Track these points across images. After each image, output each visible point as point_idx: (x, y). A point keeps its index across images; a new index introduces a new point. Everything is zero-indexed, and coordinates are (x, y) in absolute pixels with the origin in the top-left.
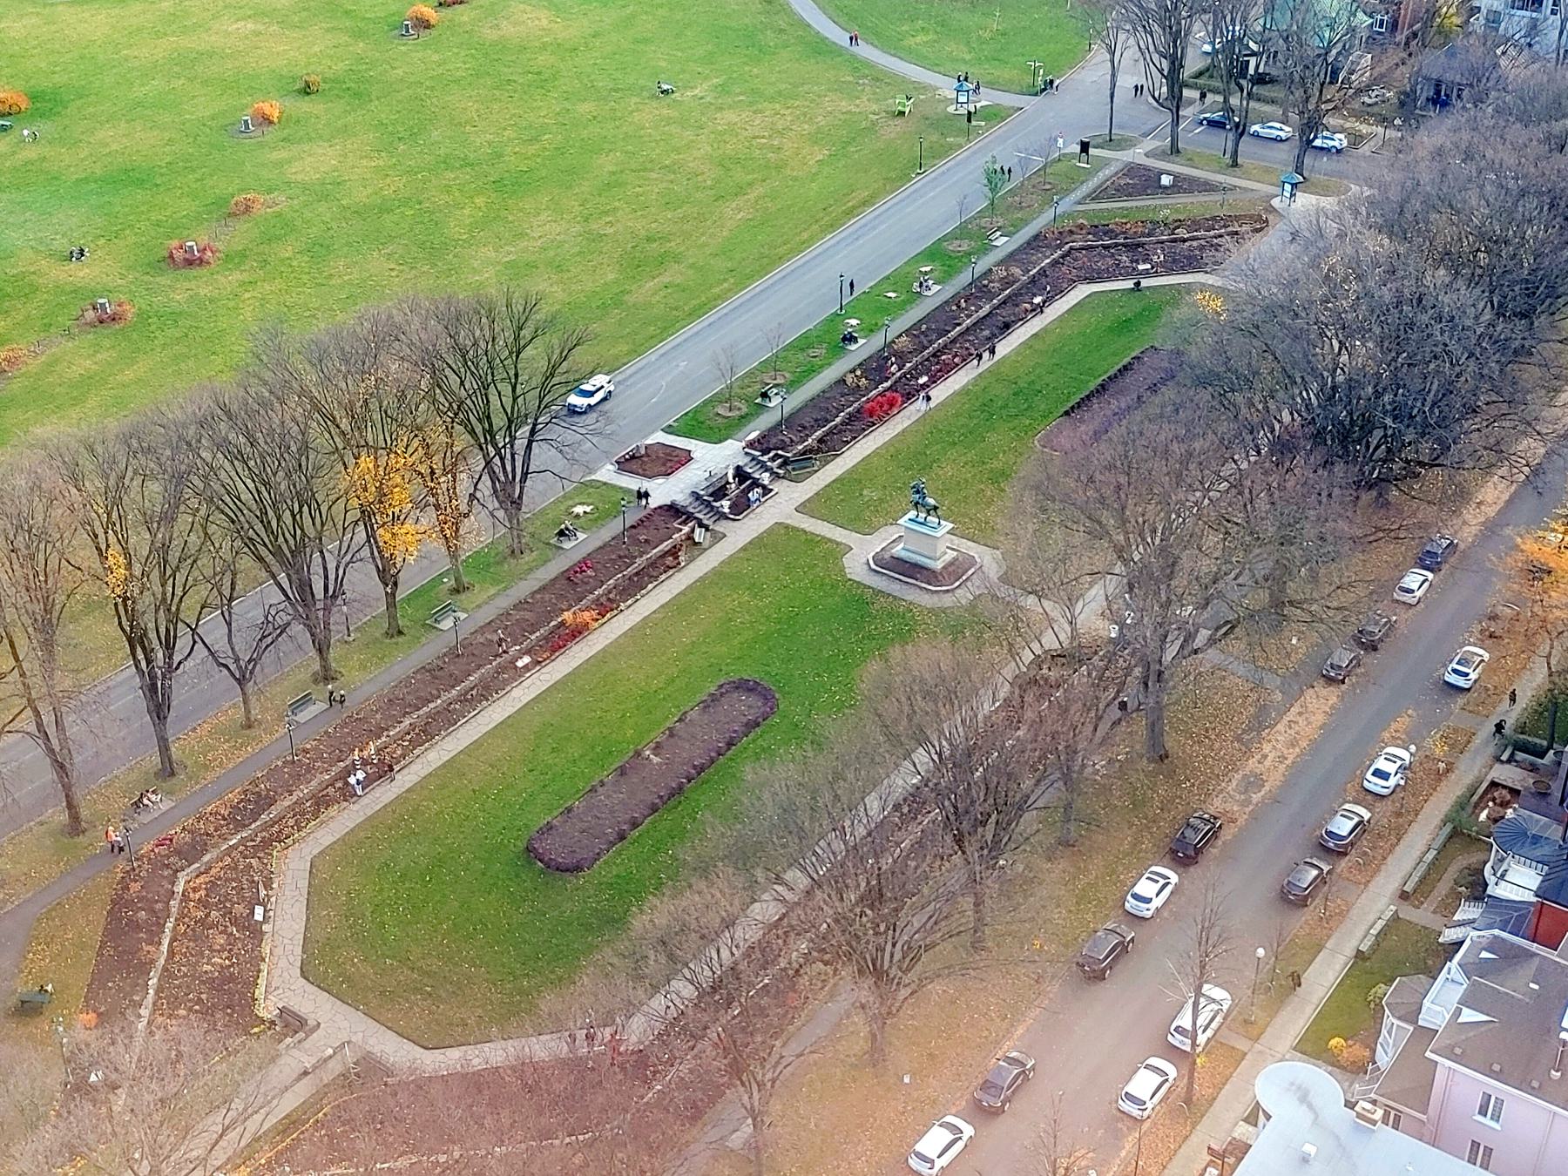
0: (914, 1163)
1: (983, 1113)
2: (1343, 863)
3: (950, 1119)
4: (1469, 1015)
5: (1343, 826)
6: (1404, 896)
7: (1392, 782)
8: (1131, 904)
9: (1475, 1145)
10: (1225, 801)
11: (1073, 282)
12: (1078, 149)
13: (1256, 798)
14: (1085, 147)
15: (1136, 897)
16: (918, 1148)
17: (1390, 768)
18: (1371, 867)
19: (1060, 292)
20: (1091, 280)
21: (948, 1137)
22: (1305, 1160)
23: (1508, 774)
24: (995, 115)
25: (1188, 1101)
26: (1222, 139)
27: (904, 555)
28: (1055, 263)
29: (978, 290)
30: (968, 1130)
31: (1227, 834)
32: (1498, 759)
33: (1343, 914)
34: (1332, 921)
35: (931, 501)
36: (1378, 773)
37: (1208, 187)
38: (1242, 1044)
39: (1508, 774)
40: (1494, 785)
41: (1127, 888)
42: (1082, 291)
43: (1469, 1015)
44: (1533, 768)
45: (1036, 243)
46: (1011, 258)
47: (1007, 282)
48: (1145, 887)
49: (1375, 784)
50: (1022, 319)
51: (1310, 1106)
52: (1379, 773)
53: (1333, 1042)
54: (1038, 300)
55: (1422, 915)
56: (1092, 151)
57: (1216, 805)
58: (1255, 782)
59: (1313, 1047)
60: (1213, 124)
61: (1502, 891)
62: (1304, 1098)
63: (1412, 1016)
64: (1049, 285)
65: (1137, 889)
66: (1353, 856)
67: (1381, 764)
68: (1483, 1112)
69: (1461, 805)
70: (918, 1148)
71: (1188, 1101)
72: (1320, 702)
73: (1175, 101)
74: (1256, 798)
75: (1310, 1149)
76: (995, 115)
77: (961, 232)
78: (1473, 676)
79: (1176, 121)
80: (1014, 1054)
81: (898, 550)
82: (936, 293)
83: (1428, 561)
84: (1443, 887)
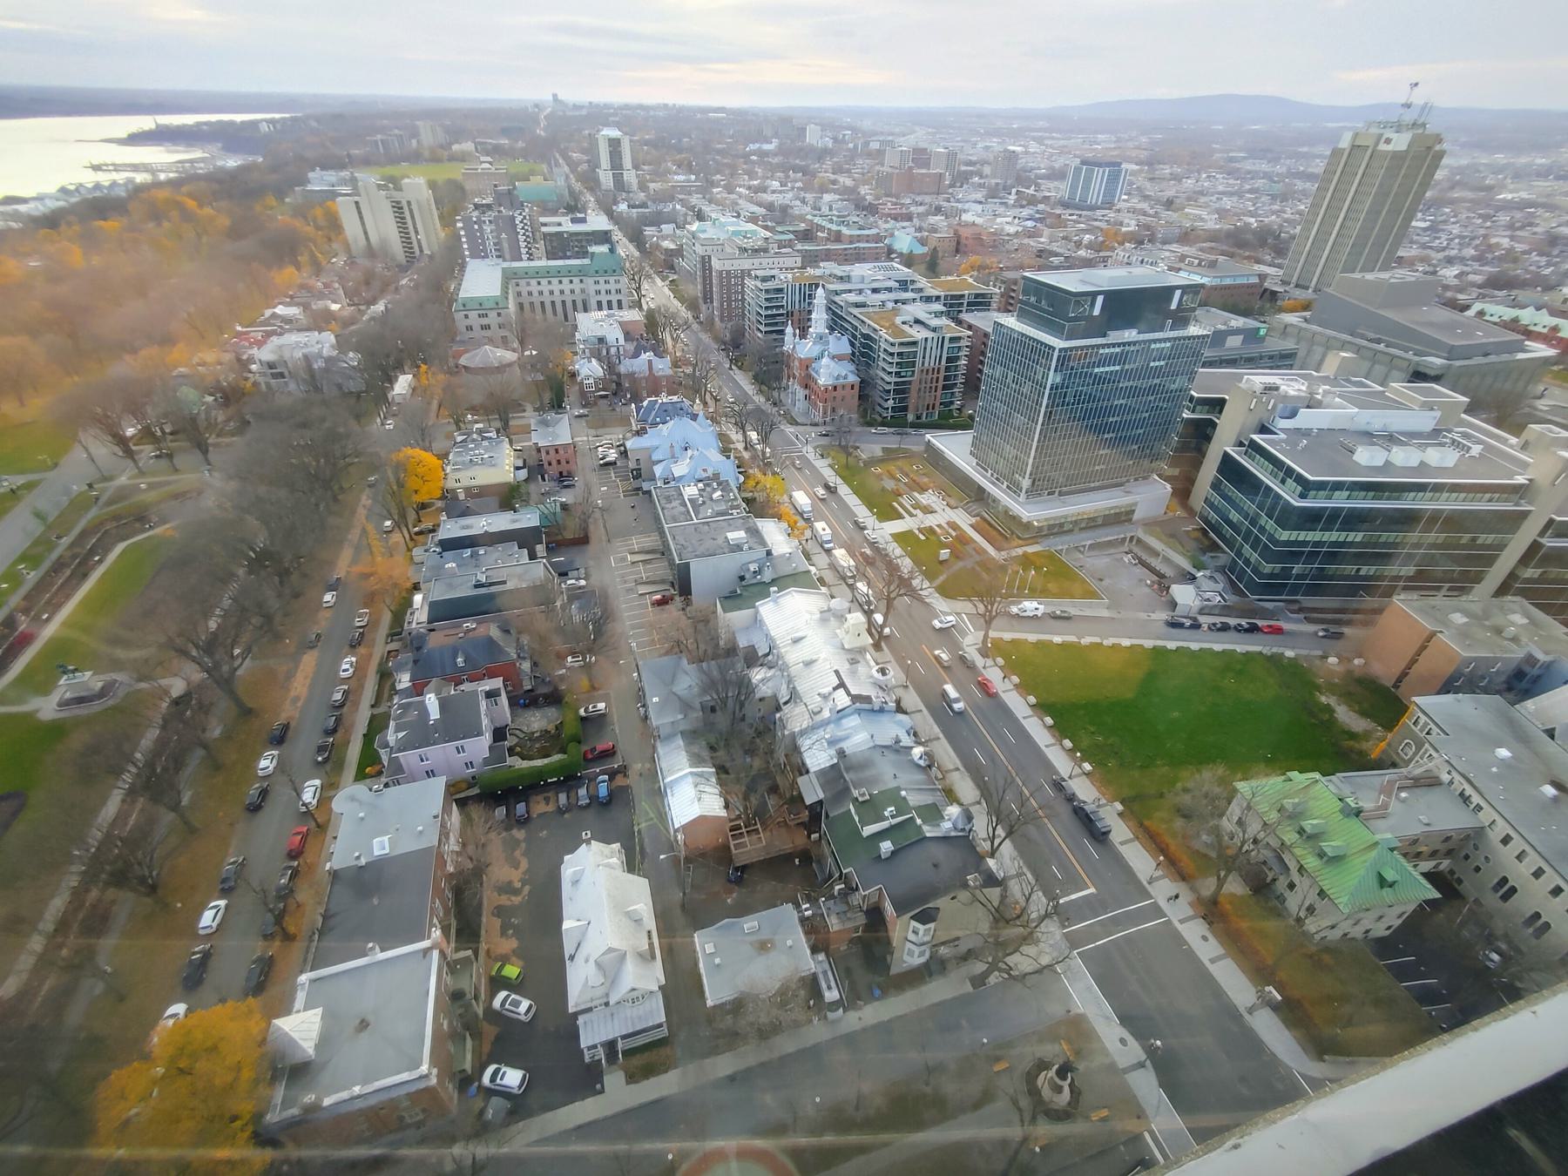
0: (202, 932)
1: (225, 892)
2: (345, 709)
3: (212, 905)
4: (401, 735)
5: (338, 696)
6: (372, 706)
7: (351, 671)
8: (260, 773)
9: (427, 772)
10: (288, 713)
11: (114, 544)
12: (87, 487)
13: (299, 704)
14: (90, 486)
15: (262, 769)
16: (201, 926)
17: (347, 666)
18: (356, 704)
19: (107, 551)
20: (123, 540)
21: (214, 911)
22: (362, 819)
23: (393, 646)
24: (30, 486)
25: (318, 826)
26: (164, 463)
27: (72, 696)
28: (98, 540)
29: (58, 566)
30: (222, 903)
31: (293, 724)
32: (387, 643)
33: (352, 726)
34: (348, 732)
35: (71, 668)
36: (344, 671)
37: (168, 483)
38: (331, 793)
39: (393, 646)
40: (389, 652)
41: (255, 768)
42: (120, 547)
43: (401, 735)
44: (400, 640)
45: (84, 534)
46: (72, 545)
47: (74, 557)
48: (263, 763)
49: (343, 675)
50: (93, 568)
51: (357, 800)
52: (344, 671)
53: (367, 770)
54: (97, 558)
55: (377, 711)
56: (95, 486)
57: (282, 719)
58: (297, 698)
59: (361, 776)
60: (156, 457)
61: (400, 687)
62: (352, 799)
63: (386, 745)
64: (103, 548)
65: (261, 767)
66: (348, 704)
67: (345, 667)
68: (422, 761)
69: (380, 665)
70: (201, 926)
71: (318, 826)
72: (309, 660)
73: (129, 454)
74: (299, 704)
75: (361, 815)
76: (30, 486)
77: (36, 543)
78: (366, 620)
79: (134, 461)
80: (232, 860)
81: (68, 695)
82: (32, 577)
83: (330, 588)
84: (386, 695)
